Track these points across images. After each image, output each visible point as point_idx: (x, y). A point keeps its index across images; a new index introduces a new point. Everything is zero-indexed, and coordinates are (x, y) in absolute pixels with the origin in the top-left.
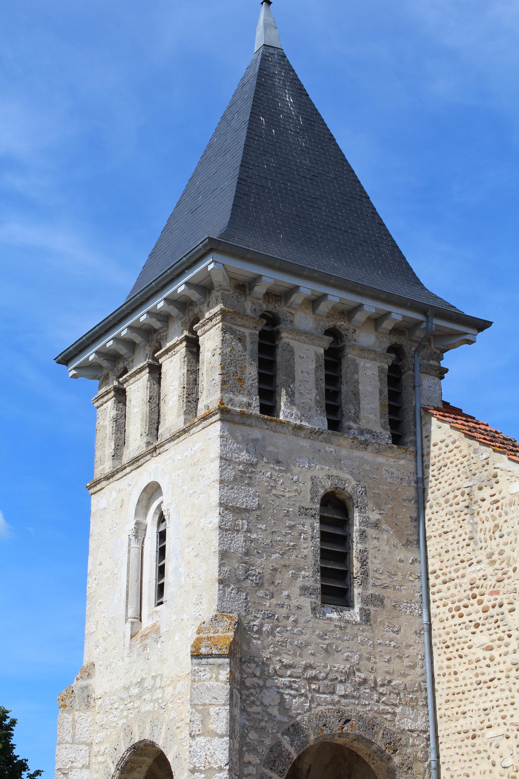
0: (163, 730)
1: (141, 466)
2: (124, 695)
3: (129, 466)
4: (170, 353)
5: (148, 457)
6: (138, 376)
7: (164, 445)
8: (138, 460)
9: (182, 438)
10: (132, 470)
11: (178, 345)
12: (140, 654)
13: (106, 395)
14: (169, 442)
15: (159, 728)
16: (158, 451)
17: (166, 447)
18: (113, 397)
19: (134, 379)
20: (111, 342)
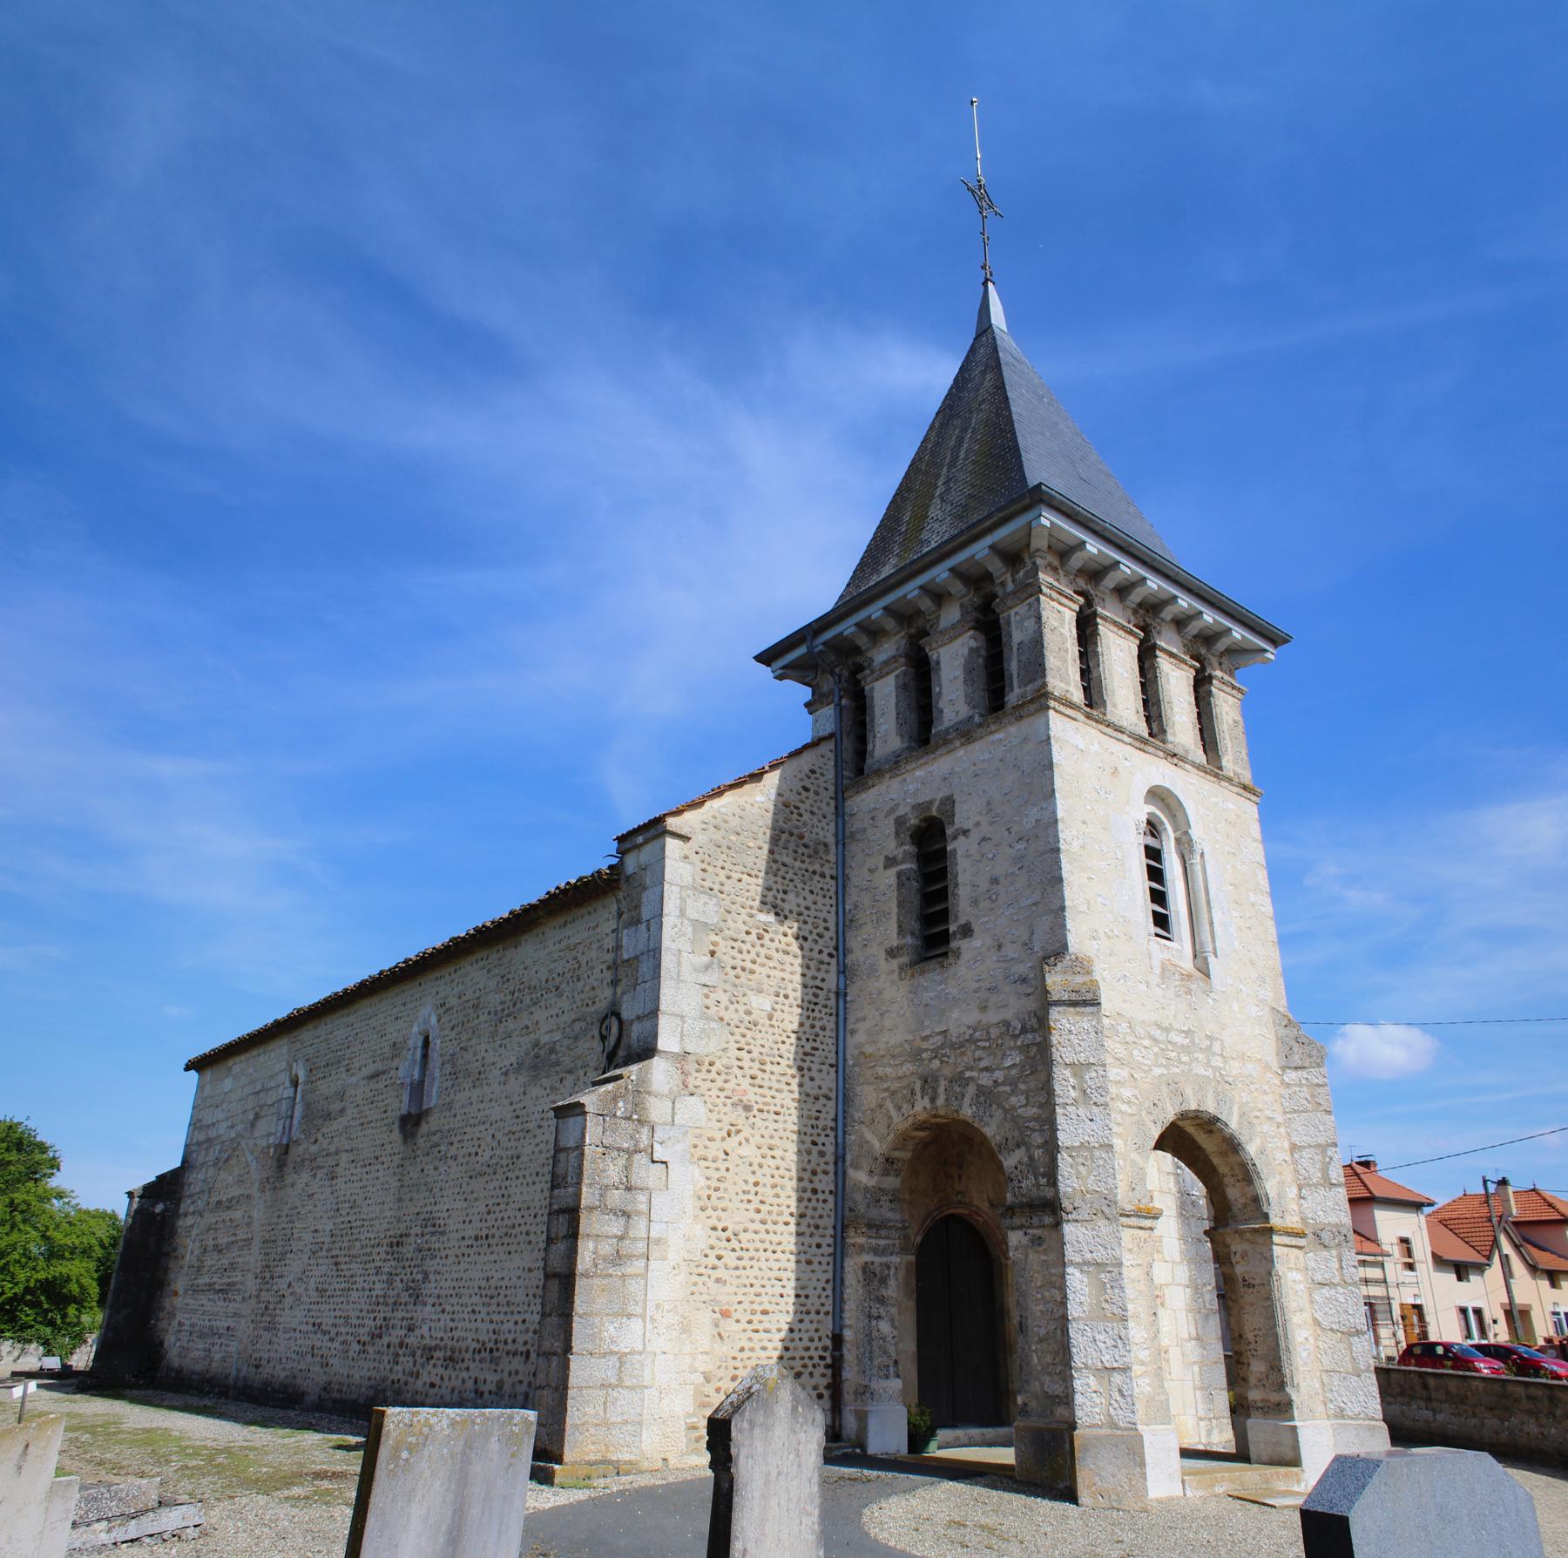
0: (1235, 1108)
1: (1144, 751)
2: (1158, 1033)
3: (1130, 737)
4: (1172, 660)
5: (1161, 754)
6: (1121, 632)
7: (1186, 763)
8: (1145, 744)
9: (1208, 777)
10: (1131, 744)
11: (1186, 664)
12: (1180, 996)
13: (1067, 597)
14: (1193, 766)
15: (1227, 1106)
16: (1175, 761)
17: (1188, 767)
18: (1074, 611)
19: (1115, 629)
20: (1128, 571)
